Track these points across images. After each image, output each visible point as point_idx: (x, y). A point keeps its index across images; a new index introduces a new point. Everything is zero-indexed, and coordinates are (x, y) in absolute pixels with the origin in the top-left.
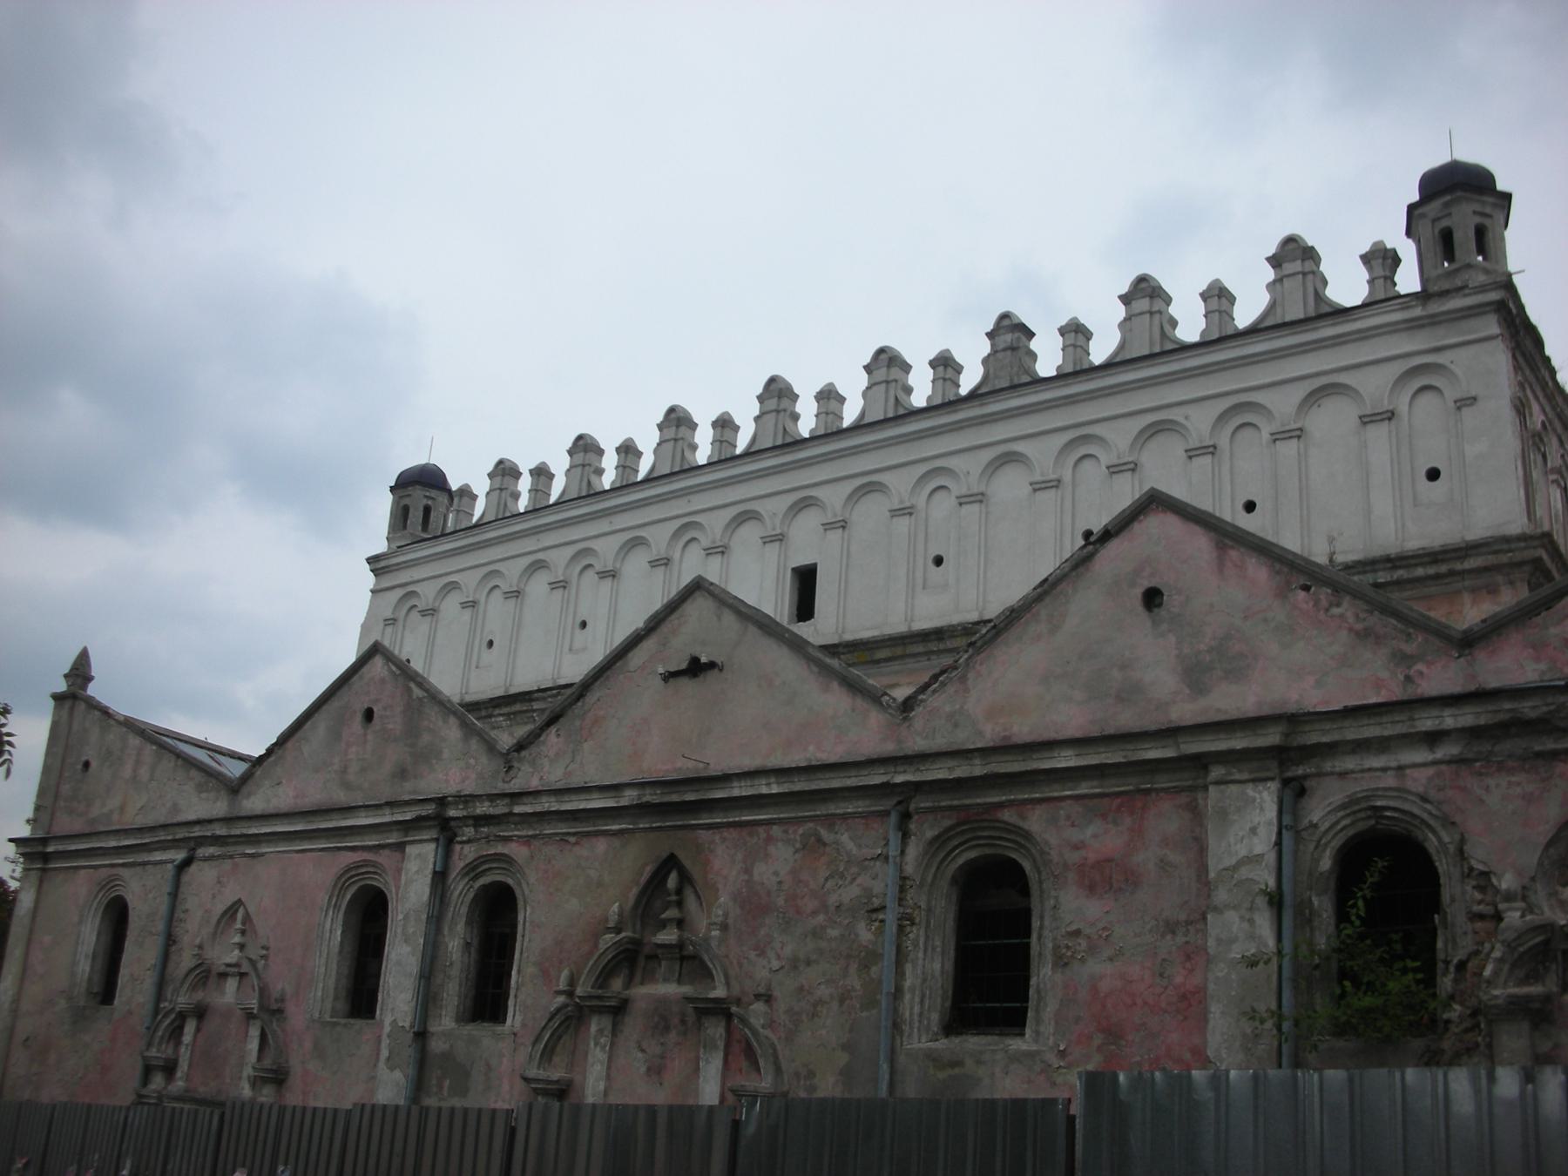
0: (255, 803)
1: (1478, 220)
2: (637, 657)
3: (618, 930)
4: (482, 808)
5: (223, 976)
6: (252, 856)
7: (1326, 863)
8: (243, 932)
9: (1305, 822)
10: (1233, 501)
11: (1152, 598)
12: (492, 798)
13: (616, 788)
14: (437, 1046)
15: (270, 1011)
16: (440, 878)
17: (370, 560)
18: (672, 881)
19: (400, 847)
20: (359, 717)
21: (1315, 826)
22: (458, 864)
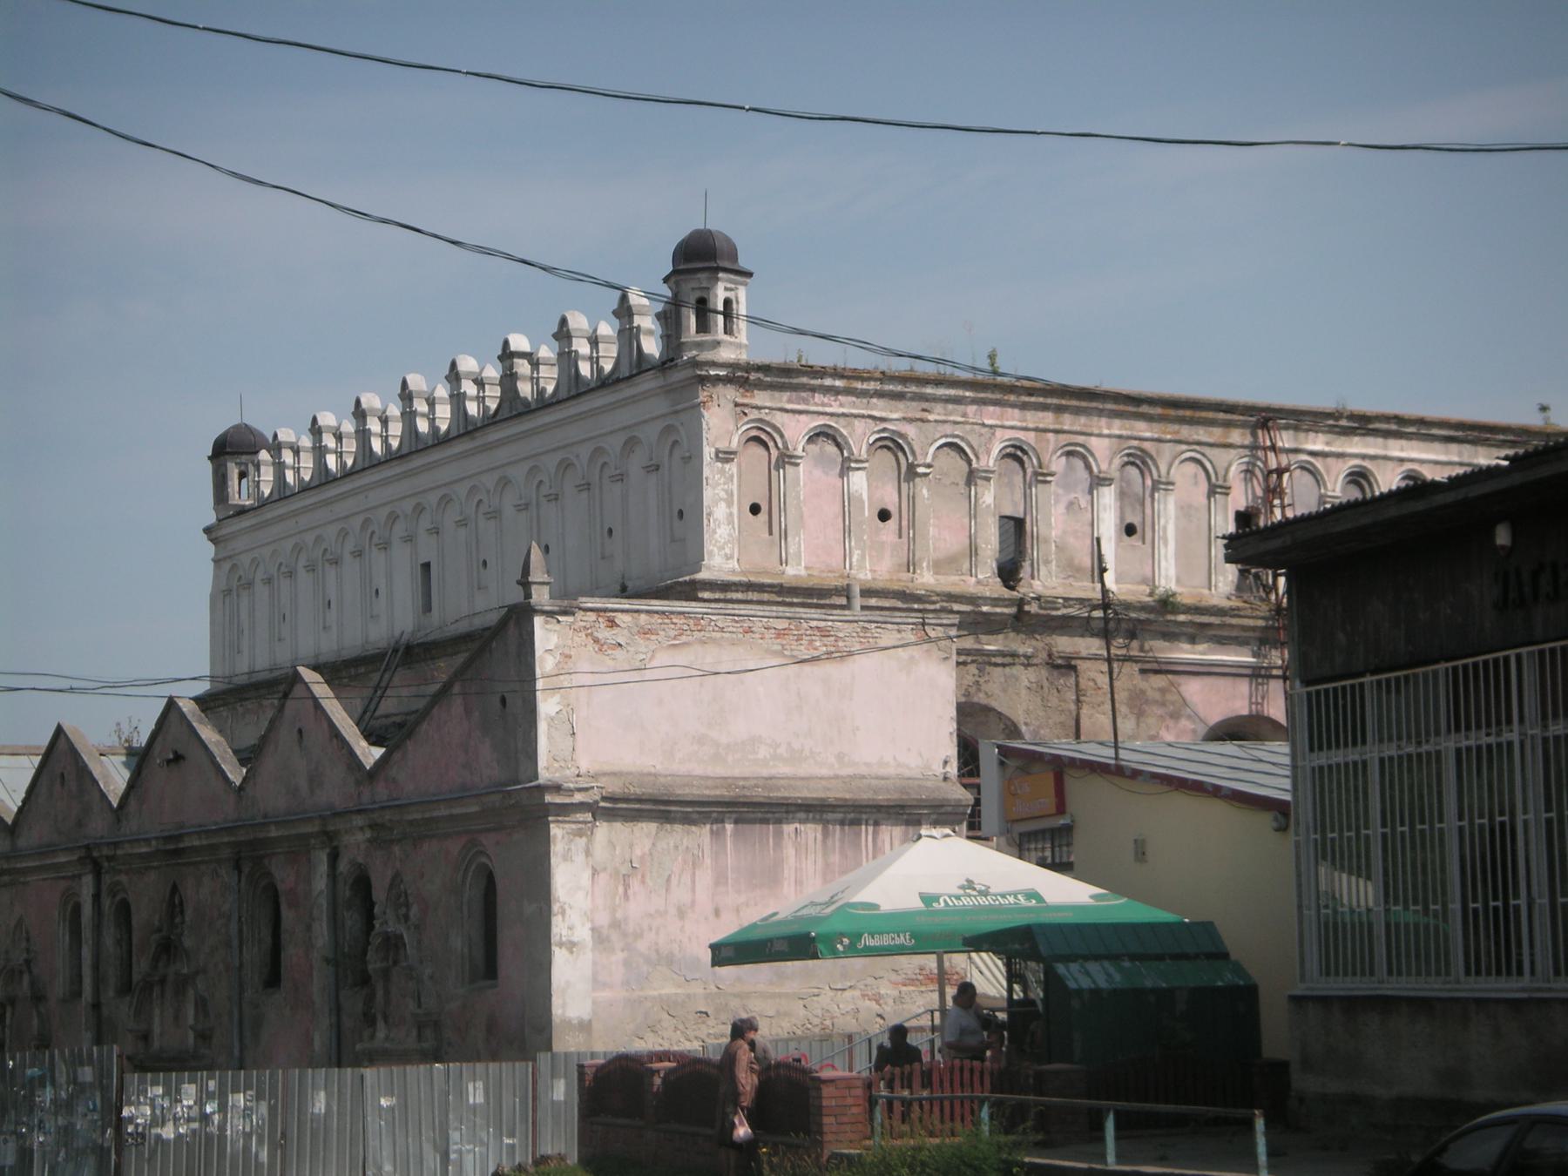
0: (26, 841)
1: (698, 294)
2: (157, 747)
3: (159, 930)
4: (106, 851)
5: (21, 972)
6: (24, 883)
7: (348, 893)
8: (28, 940)
9: (338, 872)
10: (602, 527)
11: (300, 731)
12: (109, 844)
13: (147, 841)
14: (105, 1011)
15: (38, 998)
16: (97, 897)
17: (207, 530)
18: (177, 902)
19: (80, 876)
20: (59, 780)
21: (341, 873)
22: (104, 888)
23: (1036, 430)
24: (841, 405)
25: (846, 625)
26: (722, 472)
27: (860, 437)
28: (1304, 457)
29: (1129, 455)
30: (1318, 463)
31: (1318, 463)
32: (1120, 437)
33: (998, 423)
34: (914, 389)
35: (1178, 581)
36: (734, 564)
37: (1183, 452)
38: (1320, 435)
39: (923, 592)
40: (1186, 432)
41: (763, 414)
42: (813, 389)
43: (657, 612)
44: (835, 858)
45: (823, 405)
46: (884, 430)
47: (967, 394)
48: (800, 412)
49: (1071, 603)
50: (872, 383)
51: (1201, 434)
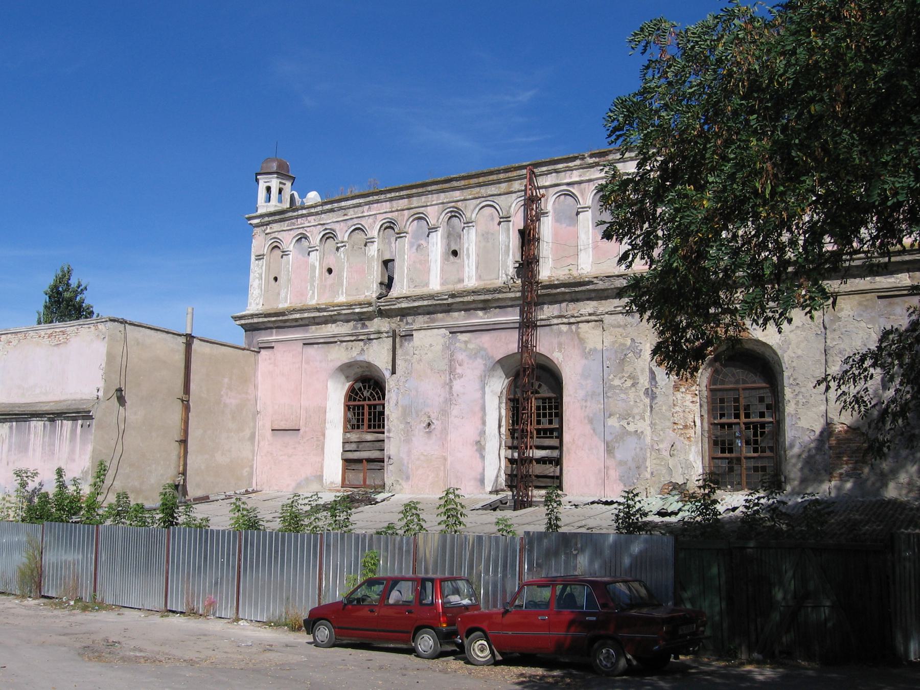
23: (397, 211)
24: (309, 222)
25: (72, 328)
26: (258, 265)
27: (315, 237)
28: (564, 187)
29: (451, 212)
30: (574, 190)
31: (574, 190)
32: (443, 203)
33: (378, 212)
34: (336, 205)
35: (479, 278)
36: (260, 307)
37: (480, 203)
38: (574, 171)
39: (324, 306)
40: (483, 191)
41: (274, 235)
42: (297, 217)
43: (12, 333)
44: (47, 439)
45: (301, 224)
46: (326, 229)
47: (361, 201)
48: (291, 230)
49: (401, 300)
50: (319, 207)
51: (493, 190)
